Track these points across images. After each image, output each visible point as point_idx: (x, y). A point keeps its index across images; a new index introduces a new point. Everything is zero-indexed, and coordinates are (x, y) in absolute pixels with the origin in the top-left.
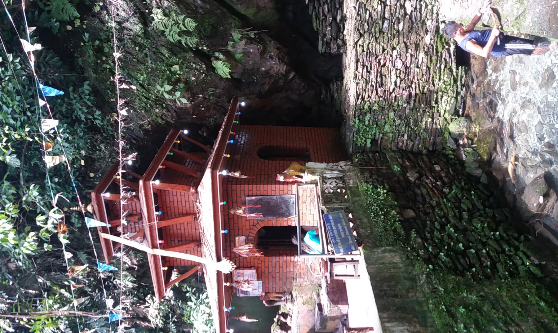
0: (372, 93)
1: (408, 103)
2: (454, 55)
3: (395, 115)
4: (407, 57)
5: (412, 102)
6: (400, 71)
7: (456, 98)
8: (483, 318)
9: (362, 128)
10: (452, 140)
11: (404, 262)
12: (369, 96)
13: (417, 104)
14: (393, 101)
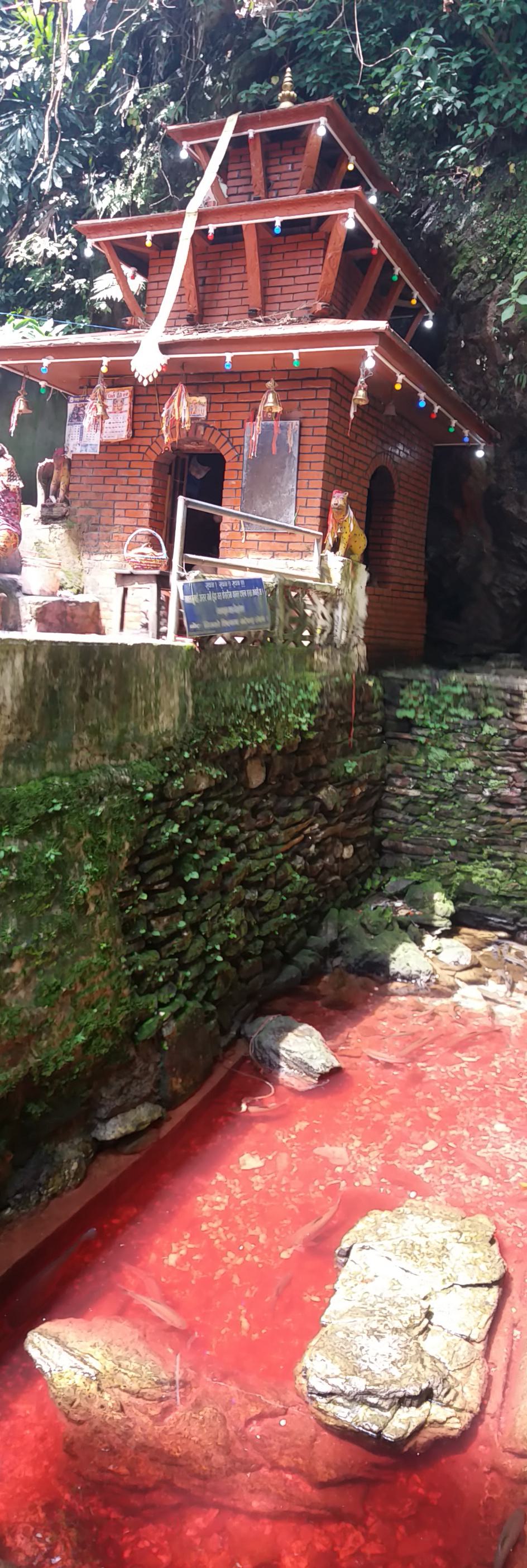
1: (491, 800)
3: (465, 771)
8: (34, 902)
10: (402, 886)
11: (159, 738)
14: (499, 768)
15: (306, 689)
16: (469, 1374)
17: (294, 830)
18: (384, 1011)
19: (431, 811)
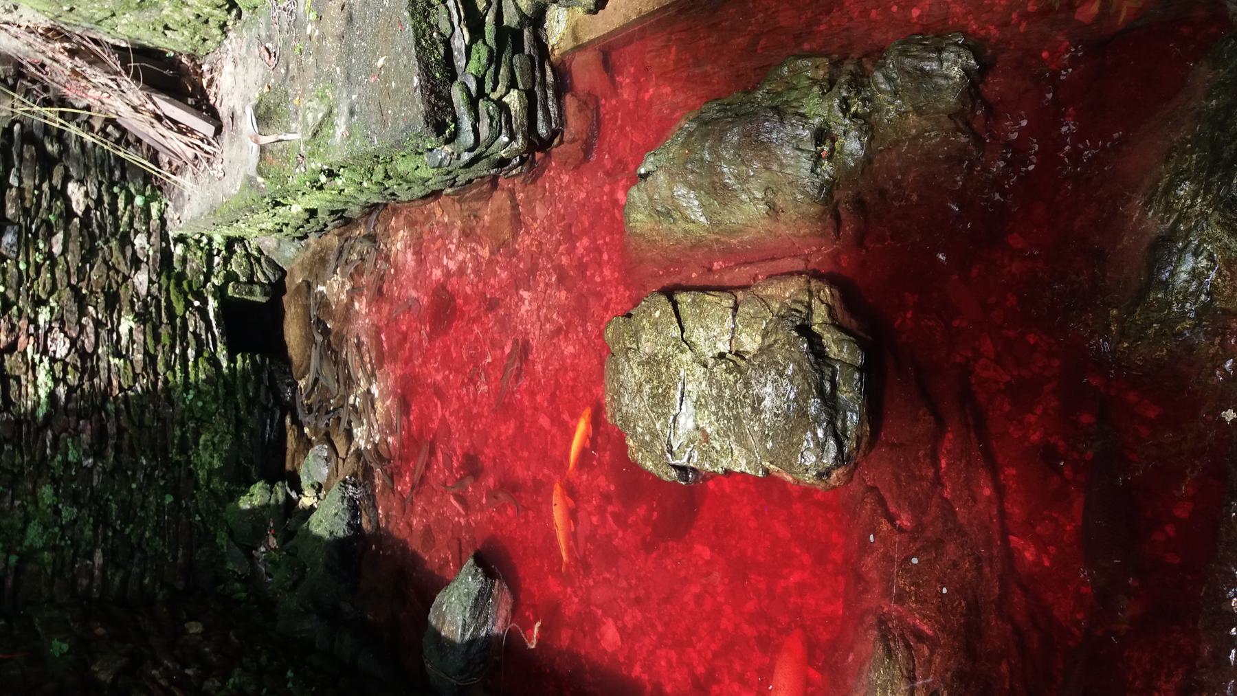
1: (99, 455)
4: (82, 328)
5: (111, 453)
6: (65, 365)
7: (237, 436)
10: (237, 551)
13: (125, 458)
16: (771, 297)
18: (398, 529)
19: (123, 530)
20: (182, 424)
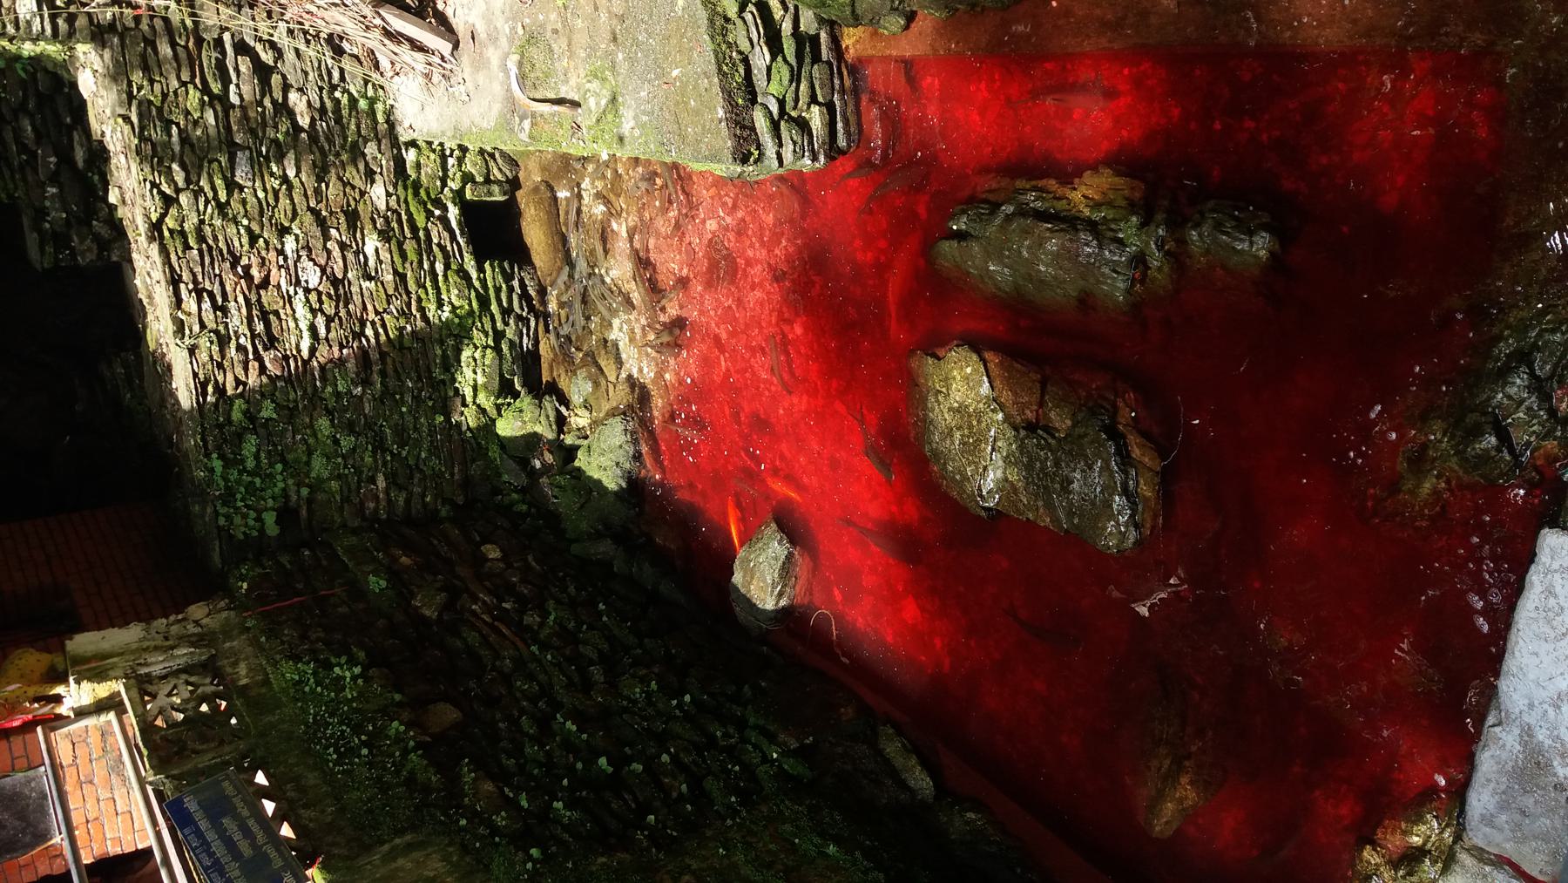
0: (246, 369)
1: (366, 382)
2: (462, 234)
3: (333, 425)
4: (329, 252)
5: (377, 379)
6: (320, 294)
7: (497, 349)
9: (239, 482)
10: (512, 464)
12: (238, 382)
13: (392, 383)
15: (300, 682)
17: (493, 638)
20: (442, 342)
